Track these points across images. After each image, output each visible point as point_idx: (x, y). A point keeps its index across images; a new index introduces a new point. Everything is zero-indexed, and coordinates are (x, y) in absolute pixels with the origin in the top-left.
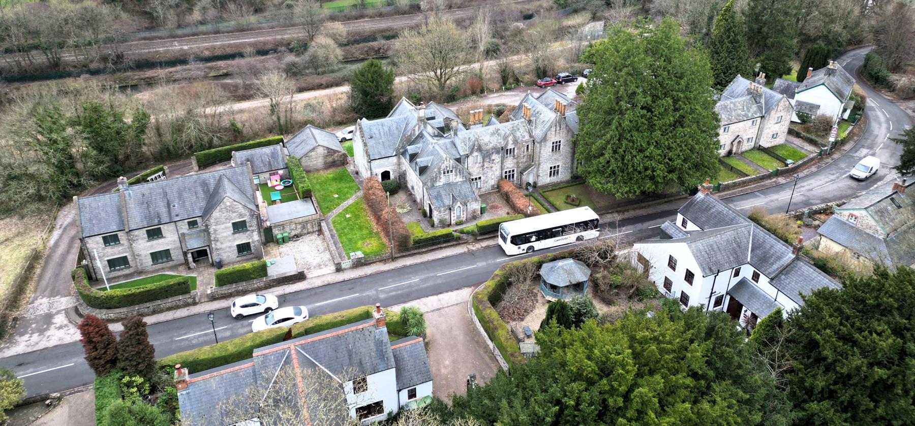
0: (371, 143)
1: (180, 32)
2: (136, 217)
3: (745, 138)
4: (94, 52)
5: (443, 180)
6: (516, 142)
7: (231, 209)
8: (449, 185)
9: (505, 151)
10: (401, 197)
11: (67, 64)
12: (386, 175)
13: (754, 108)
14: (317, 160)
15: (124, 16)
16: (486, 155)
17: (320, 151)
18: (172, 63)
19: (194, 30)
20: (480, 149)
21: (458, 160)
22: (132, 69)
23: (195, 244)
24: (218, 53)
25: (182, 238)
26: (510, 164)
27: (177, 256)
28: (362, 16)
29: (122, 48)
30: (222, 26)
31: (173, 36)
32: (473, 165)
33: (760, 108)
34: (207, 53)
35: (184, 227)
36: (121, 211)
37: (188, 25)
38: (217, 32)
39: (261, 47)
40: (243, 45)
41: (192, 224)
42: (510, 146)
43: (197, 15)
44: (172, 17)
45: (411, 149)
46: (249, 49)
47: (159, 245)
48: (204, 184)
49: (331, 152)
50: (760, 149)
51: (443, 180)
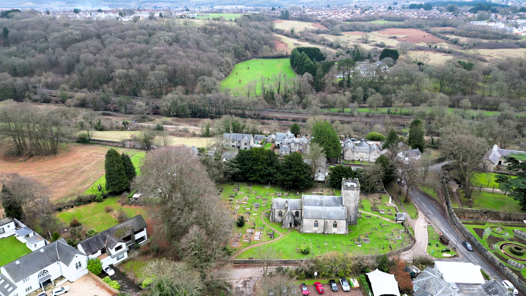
0: (277, 137)
1: (279, 111)
2: (231, 138)
3: (364, 157)
4: (253, 113)
5: (284, 146)
6: (302, 143)
7: (245, 140)
8: (285, 147)
9: (299, 144)
10: (278, 149)
11: (246, 114)
12: (278, 145)
13: (369, 150)
14: (270, 140)
15: (266, 103)
16: (296, 144)
17: (271, 138)
18: (269, 119)
19: (284, 111)
20: (294, 142)
21: (289, 143)
22: (261, 119)
23: (238, 145)
24: (285, 119)
25: (237, 144)
26: (301, 148)
27: (235, 146)
28: (338, 115)
29: (260, 112)
30: (292, 111)
31: (277, 112)
32: (292, 145)
33: (370, 151)
34: (282, 118)
35: (238, 142)
36: (230, 137)
37: (282, 109)
38: (290, 112)
39: (295, 119)
40: (289, 117)
41: (239, 142)
42: (301, 143)
43: (286, 107)
44: (279, 105)
45: (282, 139)
46: (290, 119)
47: (233, 144)
48: (243, 136)
49: (273, 139)
50: (369, 161)
51: (284, 146)
